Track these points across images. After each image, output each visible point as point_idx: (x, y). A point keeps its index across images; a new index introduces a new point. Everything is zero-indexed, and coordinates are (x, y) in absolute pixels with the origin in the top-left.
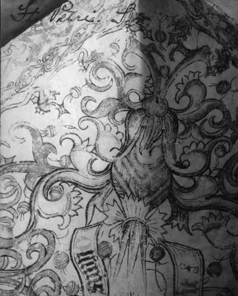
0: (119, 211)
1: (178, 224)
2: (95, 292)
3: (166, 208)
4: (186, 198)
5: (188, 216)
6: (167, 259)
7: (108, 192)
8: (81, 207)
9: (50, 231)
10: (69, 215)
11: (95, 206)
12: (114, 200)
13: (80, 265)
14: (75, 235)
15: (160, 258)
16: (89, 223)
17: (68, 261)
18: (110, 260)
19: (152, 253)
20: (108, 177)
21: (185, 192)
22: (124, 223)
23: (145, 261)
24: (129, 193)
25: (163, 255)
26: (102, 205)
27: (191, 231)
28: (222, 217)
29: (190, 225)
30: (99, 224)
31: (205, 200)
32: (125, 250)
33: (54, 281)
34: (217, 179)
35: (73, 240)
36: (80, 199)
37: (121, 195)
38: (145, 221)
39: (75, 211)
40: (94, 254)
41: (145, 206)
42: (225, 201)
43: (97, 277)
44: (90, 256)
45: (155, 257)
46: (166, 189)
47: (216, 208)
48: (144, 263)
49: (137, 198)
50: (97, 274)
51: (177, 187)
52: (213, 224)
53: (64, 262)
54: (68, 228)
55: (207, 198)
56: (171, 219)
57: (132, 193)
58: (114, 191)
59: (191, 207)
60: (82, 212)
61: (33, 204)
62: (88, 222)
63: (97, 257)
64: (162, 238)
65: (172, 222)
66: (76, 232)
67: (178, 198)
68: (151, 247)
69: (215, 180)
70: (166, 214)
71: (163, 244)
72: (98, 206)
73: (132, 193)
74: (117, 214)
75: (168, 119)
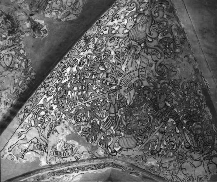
1: (144, 51)
6: (139, 59)
11: (122, 43)
20: (128, 34)
25: (138, 58)
29: (148, 52)
30: (122, 47)
33: (109, 62)
43: (119, 61)
50: (120, 60)
55: (155, 46)
56: (143, 48)
57: (134, 39)
60: (118, 44)
72: (123, 43)
75: (150, 18)
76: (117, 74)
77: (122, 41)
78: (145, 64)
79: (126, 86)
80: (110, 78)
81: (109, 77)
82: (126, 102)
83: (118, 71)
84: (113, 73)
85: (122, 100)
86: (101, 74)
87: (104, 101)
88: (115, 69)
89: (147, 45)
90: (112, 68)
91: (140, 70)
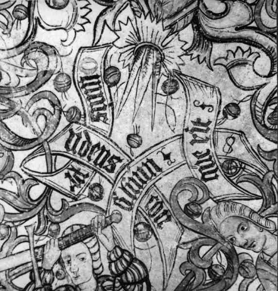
0: (133, 31)
2: (99, 121)
3: (188, 34)
4: (211, 26)
5: (212, 48)
6: (180, 92)
7: (122, 6)
8: (89, 22)
9: (52, 47)
10: (74, 29)
11: (105, 22)
12: (128, 18)
13: (83, 90)
14: (80, 54)
15: (173, 92)
16: (97, 43)
17: (70, 84)
18: (118, 88)
19: (164, 85)
21: (212, 19)
22: (138, 47)
23: (156, 93)
24: (146, 11)
26: (114, 22)
27: (212, 64)
28: (251, 54)
30: (108, 46)
31: (235, 31)
32: (135, 79)
33: (53, 105)
34: (253, 7)
35: (77, 60)
36: (88, 10)
37: (137, 13)
38: (161, 48)
39: (82, 25)
40: (100, 79)
41: (164, 30)
42: (259, 35)
44: (95, 80)
45: (167, 90)
46: (191, 12)
47: (246, 42)
48: (154, 95)
49: (155, 19)
51: (204, 11)
52: (239, 60)
53: (66, 85)
54: (72, 45)
55: (237, 29)
56: (190, 49)
57: (150, 12)
58: (129, 6)
59: (217, 37)
60: (89, 27)
61: (32, 8)
62: (95, 42)
63: (103, 83)
64: (177, 69)
65: (191, 52)
66: (81, 51)
67: (204, 26)
68: (164, 79)
69: (251, 8)
70: (186, 43)
71: (178, 77)
72: (110, 22)
73: (150, 12)
74: (129, 36)
76: (94, 157)
77: (101, 14)
78: (207, 109)
79: (137, 210)
80: (62, 175)
81: (57, 171)
82: (146, 279)
83: (98, 145)
84: (78, 157)
85: (126, 270)
86: (20, 156)
87: (39, 283)
88: (84, 138)
89: (205, 27)
90: (71, 131)
91: (189, 137)
